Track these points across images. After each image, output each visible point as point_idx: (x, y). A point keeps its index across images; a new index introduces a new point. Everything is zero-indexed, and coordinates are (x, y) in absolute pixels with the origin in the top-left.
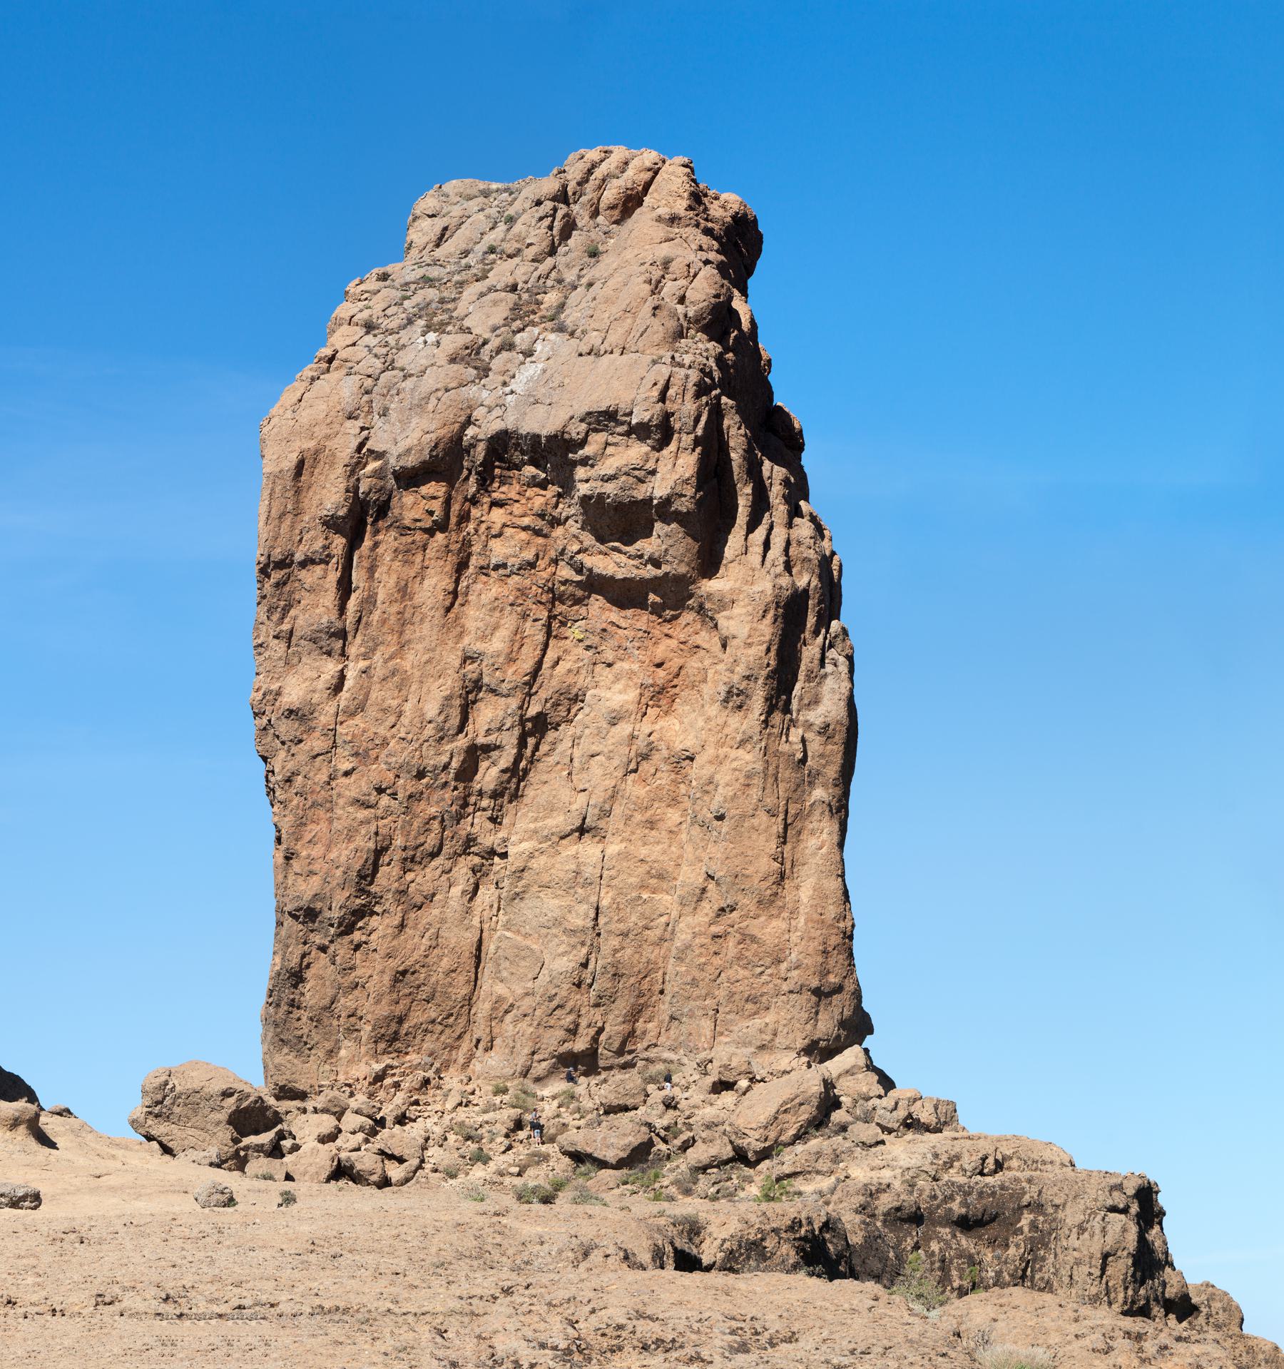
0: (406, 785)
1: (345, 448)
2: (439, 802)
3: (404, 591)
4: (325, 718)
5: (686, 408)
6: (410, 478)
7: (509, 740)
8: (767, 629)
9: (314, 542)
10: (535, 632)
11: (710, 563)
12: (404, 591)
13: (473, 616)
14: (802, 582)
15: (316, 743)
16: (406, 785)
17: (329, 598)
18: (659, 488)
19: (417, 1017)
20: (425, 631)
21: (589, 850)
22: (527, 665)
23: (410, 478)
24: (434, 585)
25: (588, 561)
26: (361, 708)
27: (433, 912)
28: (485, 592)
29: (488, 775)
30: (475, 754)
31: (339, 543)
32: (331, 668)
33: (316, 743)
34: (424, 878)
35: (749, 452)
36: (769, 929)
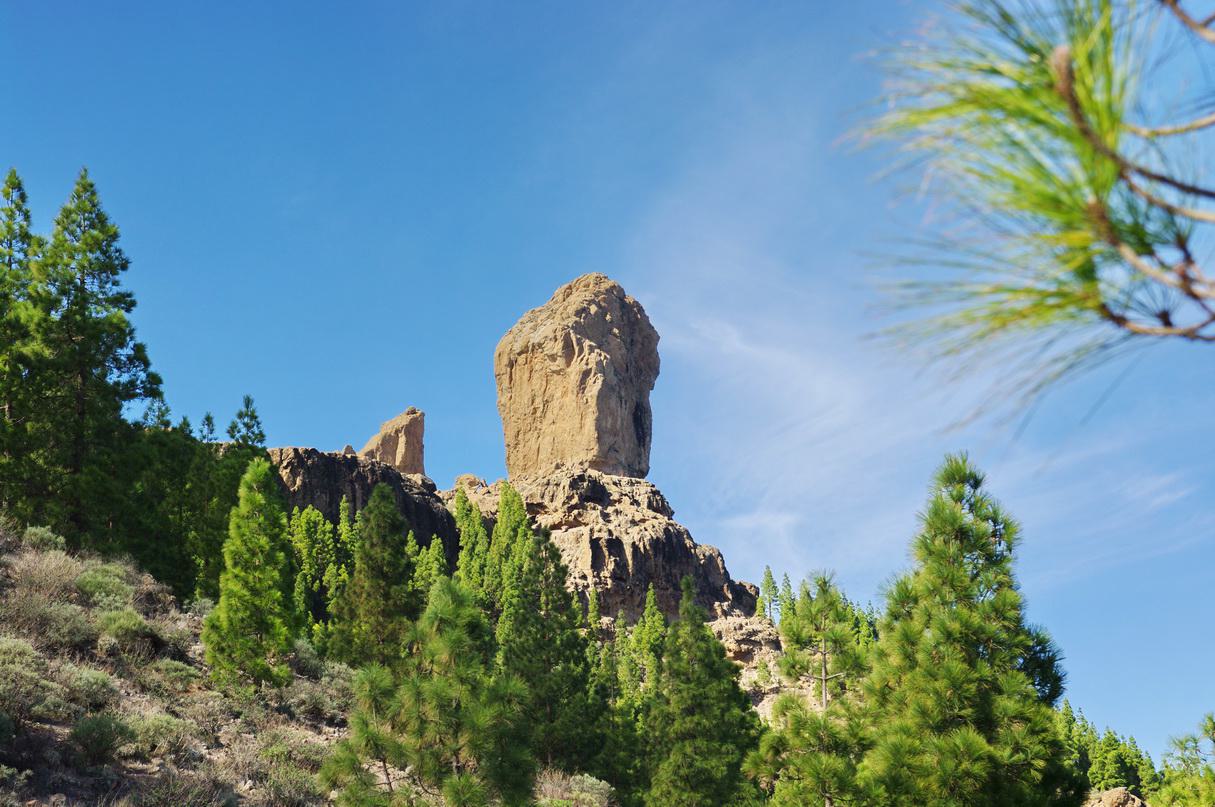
0: (523, 417)
1: (508, 350)
2: (530, 420)
3: (521, 378)
4: (508, 405)
5: (559, 334)
6: (519, 354)
7: (541, 406)
8: (578, 378)
9: (503, 371)
10: (544, 383)
11: (568, 364)
12: (521, 378)
13: (534, 381)
14: (589, 367)
15: (507, 411)
16: (523, 417)
17: (508, 381)
18: (555, 351)
19: (530, 464)
20: (525, 385)
21: (553, 427)
22: (543, 390)
23: (519, 354)
24: (527, 375)
25: (552, 367)
26: (514, 402)
27: (530, 443)
28: (536, 376)
29: (538, 414)
30: (535, 412)
31: (509, 369)
32: (509, 395)
33: (507, 411)
34: (528, 436)
35: (578, 340)
36: (578, 438)
